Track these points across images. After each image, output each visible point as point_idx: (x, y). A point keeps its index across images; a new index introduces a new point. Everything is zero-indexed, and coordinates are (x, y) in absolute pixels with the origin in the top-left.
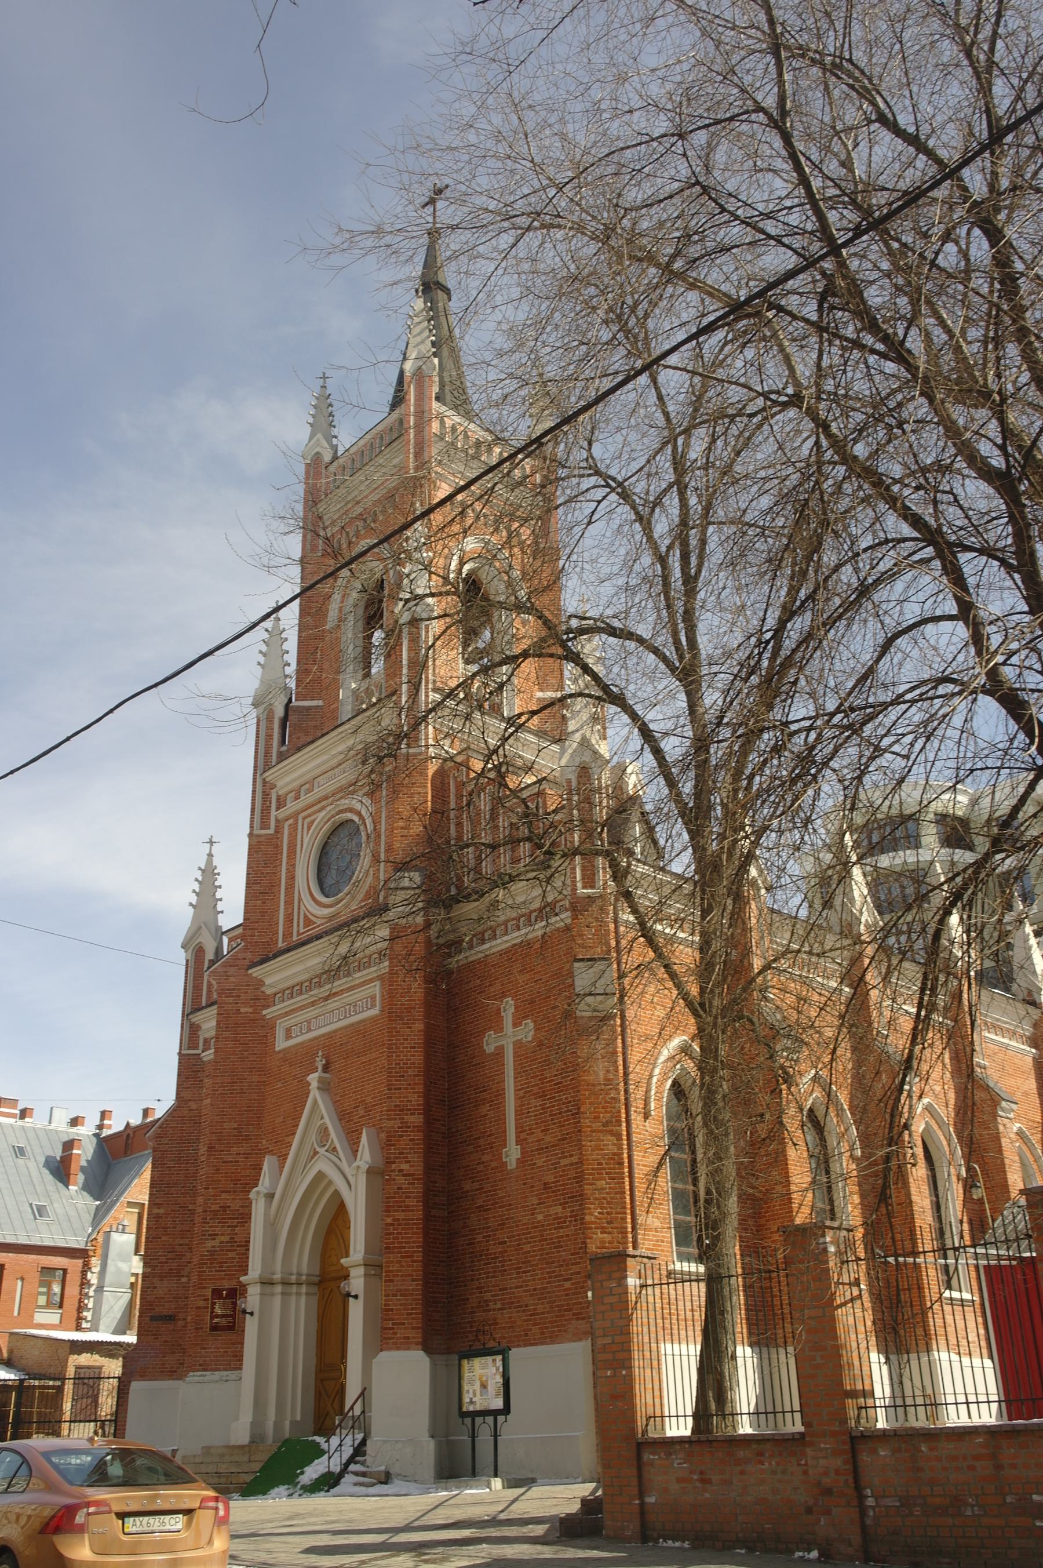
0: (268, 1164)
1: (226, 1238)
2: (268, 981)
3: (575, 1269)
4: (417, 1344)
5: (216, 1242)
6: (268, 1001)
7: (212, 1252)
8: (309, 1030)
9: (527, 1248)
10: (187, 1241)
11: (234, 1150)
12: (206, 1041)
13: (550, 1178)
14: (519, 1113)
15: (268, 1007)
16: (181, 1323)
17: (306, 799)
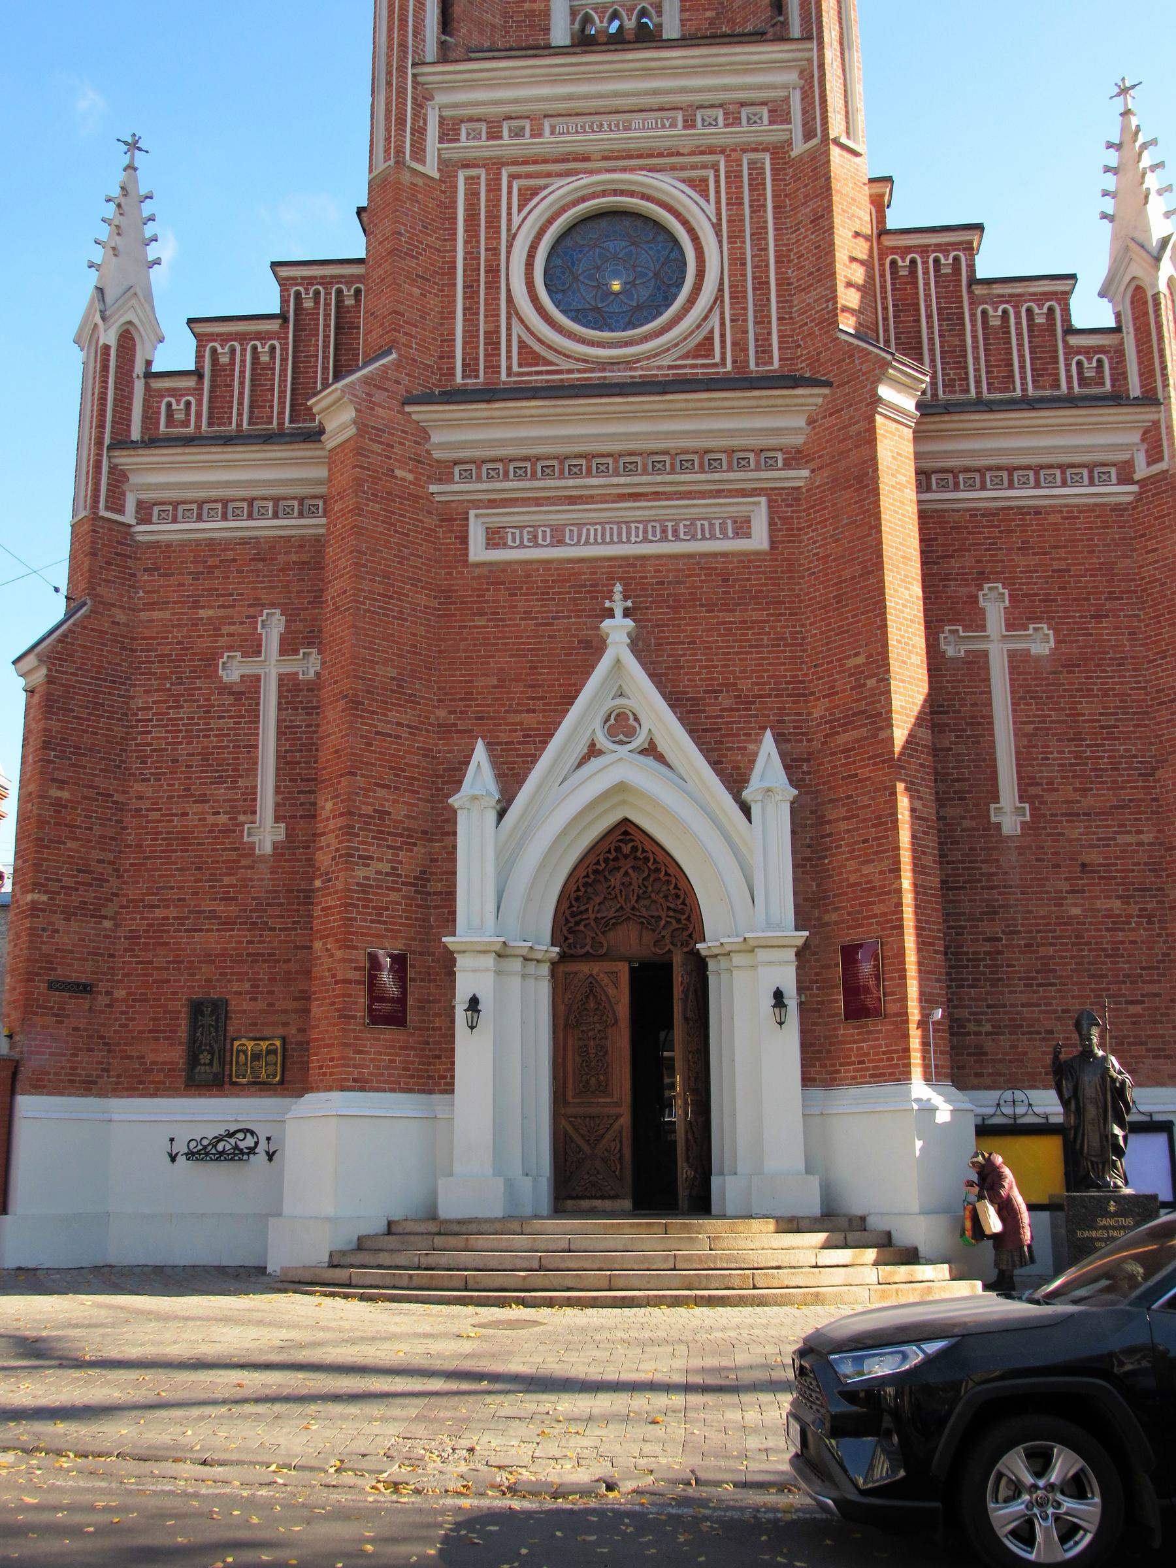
0: (480, 753)
1: (386, 867)
2: (436, 437)
3: (1148, 988)
4: (946, 1076)
5: (370, 872)
6: (443, 471)
7: (365, 887)
8: (560, 542)
9: (1043, 952)
10: (111, 856)
11: (393, 716)
12: (140, 505)
13: (1093, 857)
14: (1022, 757)
15: (440, 481)
16: (102, 1000)
17: (526, 145)
